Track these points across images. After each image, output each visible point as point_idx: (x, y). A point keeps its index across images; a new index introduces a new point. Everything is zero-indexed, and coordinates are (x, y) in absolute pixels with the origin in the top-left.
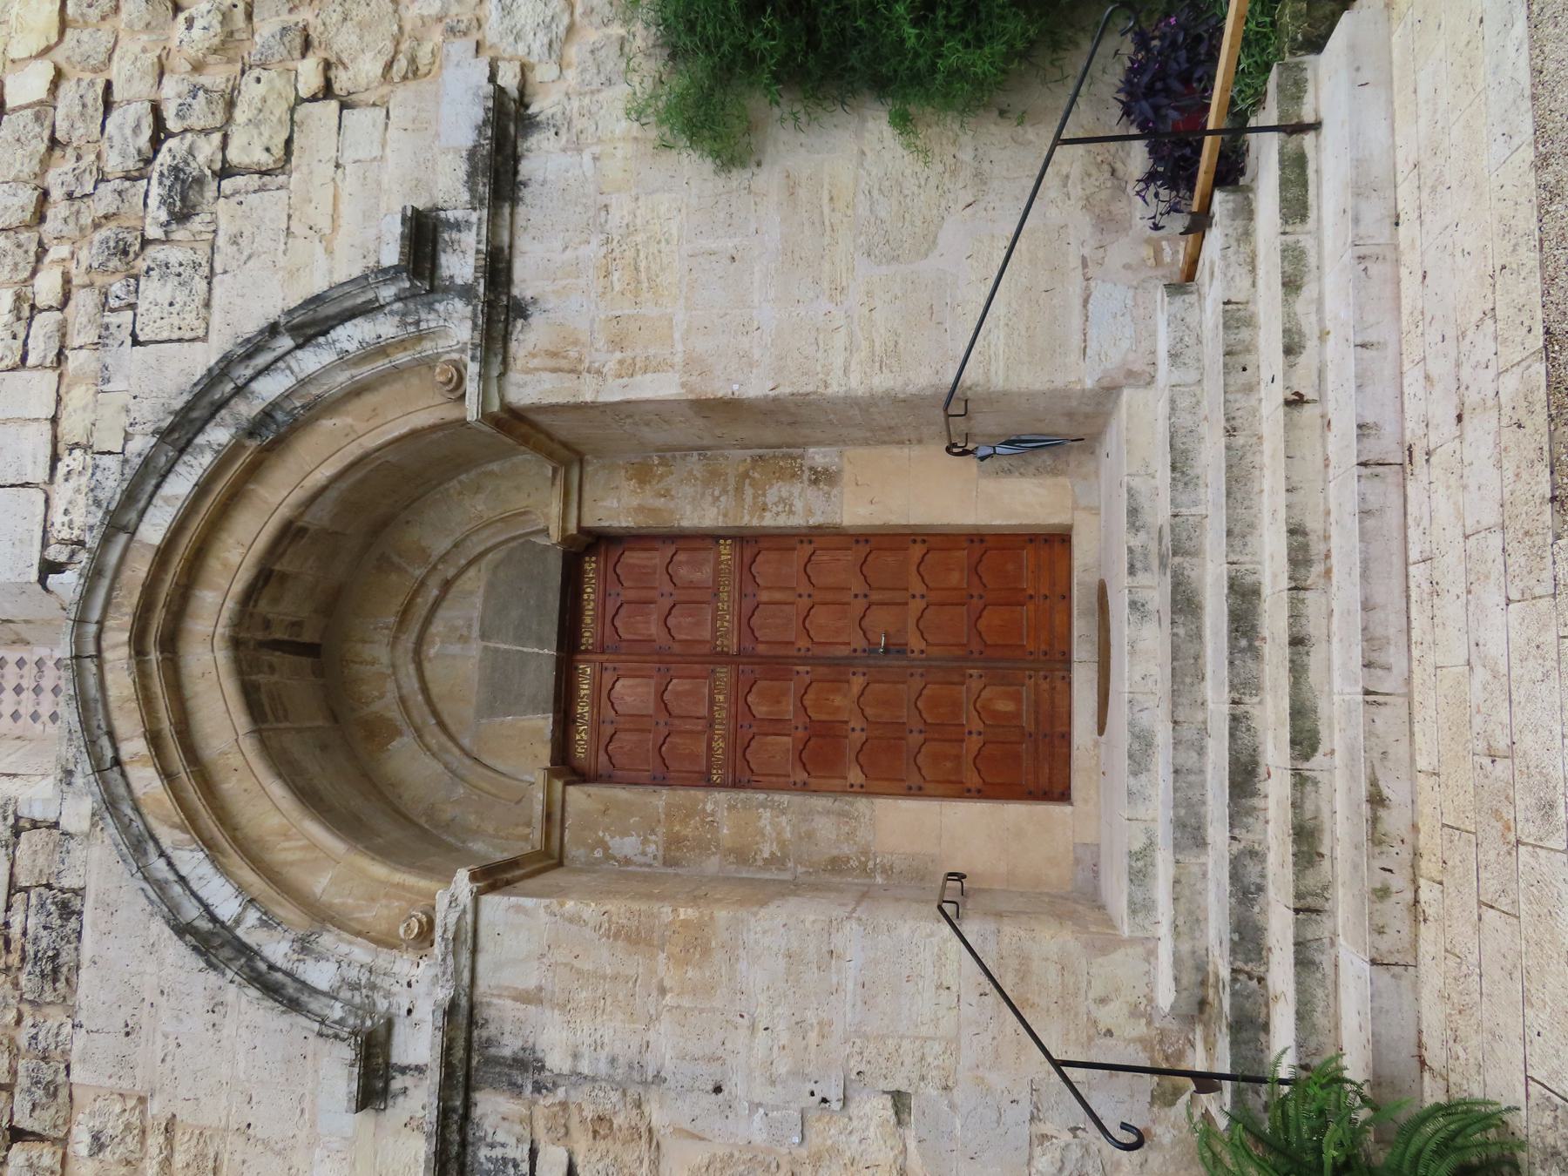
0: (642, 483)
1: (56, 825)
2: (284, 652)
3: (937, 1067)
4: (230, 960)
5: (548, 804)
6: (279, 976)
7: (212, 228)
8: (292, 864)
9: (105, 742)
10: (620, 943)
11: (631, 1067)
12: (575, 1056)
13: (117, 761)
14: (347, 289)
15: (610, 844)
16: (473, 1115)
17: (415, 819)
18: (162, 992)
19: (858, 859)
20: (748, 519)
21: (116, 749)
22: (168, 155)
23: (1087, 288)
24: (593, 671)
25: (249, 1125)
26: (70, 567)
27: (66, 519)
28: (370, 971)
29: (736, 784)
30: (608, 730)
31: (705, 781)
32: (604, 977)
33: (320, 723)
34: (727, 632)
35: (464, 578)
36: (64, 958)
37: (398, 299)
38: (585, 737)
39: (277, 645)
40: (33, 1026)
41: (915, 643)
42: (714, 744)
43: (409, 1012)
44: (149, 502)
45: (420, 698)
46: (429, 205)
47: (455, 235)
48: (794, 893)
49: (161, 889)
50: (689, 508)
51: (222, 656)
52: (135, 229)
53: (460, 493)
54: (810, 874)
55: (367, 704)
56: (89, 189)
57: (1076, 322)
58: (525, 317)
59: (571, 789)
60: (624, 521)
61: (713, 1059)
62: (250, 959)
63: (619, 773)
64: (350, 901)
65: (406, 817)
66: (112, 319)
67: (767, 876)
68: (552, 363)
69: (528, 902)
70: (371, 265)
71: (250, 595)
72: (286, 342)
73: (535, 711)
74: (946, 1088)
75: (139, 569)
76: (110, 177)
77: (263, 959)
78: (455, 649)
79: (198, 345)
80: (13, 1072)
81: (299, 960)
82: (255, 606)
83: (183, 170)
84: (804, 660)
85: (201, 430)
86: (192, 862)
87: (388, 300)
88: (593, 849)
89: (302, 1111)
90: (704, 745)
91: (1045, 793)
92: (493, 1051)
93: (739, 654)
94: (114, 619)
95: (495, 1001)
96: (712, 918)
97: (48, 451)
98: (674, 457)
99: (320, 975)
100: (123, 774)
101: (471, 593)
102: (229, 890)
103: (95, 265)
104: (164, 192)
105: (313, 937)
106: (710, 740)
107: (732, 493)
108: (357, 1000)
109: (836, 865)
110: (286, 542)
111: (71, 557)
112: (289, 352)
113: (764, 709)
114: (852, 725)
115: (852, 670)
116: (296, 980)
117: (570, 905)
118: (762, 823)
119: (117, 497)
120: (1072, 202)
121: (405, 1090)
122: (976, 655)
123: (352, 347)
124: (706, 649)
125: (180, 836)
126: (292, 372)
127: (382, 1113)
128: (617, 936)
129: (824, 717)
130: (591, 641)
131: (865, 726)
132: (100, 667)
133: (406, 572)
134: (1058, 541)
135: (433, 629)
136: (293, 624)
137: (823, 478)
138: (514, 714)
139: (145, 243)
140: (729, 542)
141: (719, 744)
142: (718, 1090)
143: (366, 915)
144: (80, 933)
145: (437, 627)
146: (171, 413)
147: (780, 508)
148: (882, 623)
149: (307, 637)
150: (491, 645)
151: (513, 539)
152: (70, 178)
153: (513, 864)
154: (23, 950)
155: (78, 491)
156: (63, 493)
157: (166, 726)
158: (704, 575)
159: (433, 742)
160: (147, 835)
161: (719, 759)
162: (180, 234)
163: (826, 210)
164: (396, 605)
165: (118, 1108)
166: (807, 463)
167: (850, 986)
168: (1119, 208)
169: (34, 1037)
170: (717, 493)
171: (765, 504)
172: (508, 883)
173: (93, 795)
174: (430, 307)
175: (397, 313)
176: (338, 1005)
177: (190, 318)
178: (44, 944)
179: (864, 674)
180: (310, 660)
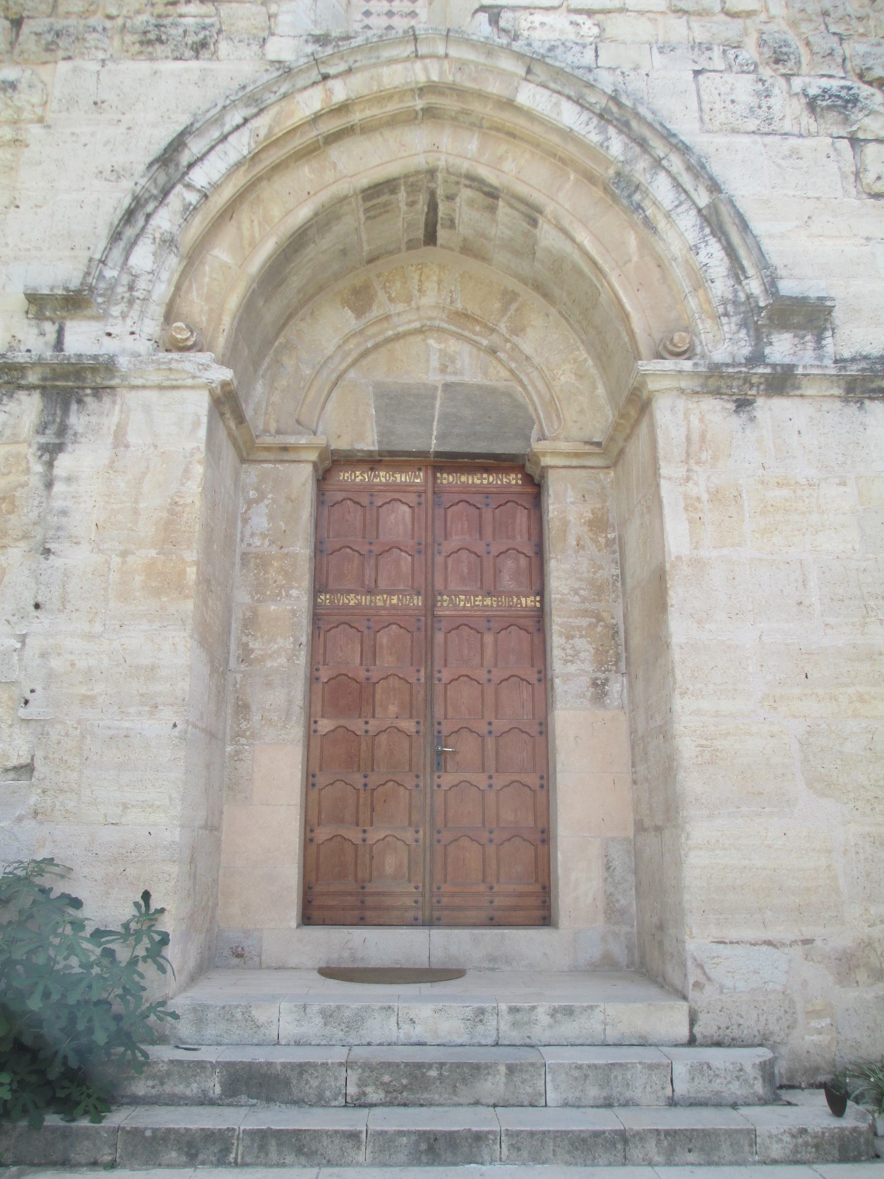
0: (590, 524)
1: (273, 34)
2: (427, 214)
3: (55, 806)
4: (155, 180)
5: (296, 448)
6: (141, 222)
7: (803, 132)
8: (239, 228)
9: (343, 67)
10: (165, 515)
11: (59, 528)
12: (69, 480)
13: (326, 77)
14: (755, 251)
15: (262, 504)
16: (20, 392)
17: (283, 333)
18: (129, 128)
19: (248, 729)
20: (557, 623)
21: (335, 77)
22: (868, 93)
23: (783, 944)
24: (417, 485)
25: (17, 207)
26: (495, 30)
27: (537, 24)
28: (144, 299)
29: (317, 617)
30: (365, 500)
31: (319, 587)
32: (136, 502)
33: (366, 248)
34: (455, 605)
35: (500, 367)
36: (159, 48)
37: (749, 297)
38: (358, 480)
39: (433, 207)
40: (104, 29)
41: (448, 779)
42: (352, 595)
43: (109, 334)
44: (554, 91)
45: (390, 333)
46: (837, 322)
47: (810, 345)
48: (214, 671)
49: (216, 120)
50: (567, 566)
51: (420, 161)
52: (799, 68)
53: (575, 360)
54: (235, 686)
55: (384, 288)
56: (833, 29)
57: (749, 934)
58: (736, 411)
59: (309, 468)
60: (553, 508)
61: (64, 601)
62: (155, 198)
63: (326, 512)
64: (207, 280)
65: (284, 325)
66: (716, 53)
67: (233, 647)
68: (695, 437)
69: (202, 432)
70: (778, 272)
71: (474, 181)
72: (703, 199)
73: (381, 434)
74: (36, 813)
75: (494, 87)
76: (845, 45)
77: (156, 208)
78: (435, 363)
79: (697, 125)
80: (68, 14)
81: (154, 239)
82: (466, 186)
83: (855, 106)
84: (430, 677)
85: (620, 132)
87: (746, 287)
88: (256, 489)
89: (29, 250)
90: (352, 587)
91: (310, 902)
92: (74, 407)
93: (434, 616)
94: (450, 68)
95: (117, 408)
96: (187, 597)
97: (596, 6)
98: (614, 552)
100: (314, 84)
101: (485, 374)
102: (215, 177)
103: (765, 37)
104: (834, 91)
105: (175, 250)
106: (357, 593)
107: (583, 606)
108: (120, 290)
109: (243, 709)
110: (522, 208)
111: (504, 30)
112: (694, 203)
113: (385, 641)
114: (372, 722)
115: (422, 721)
116: (138, 236)
117: (199, 470)
118: (280, 640)
119: (557, 64)
120: (867, 930)
121: (43, 334)
122: (436, 836)
123: (702, 257)
124: (439, 585)
125: (263, 133)
126: (677, 206)
127: (24, 315)
128: (171, 512)
129: (378, 696)
130: (445, 482)
131: (370, 734)
132: (407, 59)
133: (503, 316)
135: (452, 341)
136: (452, 221)
137: (599, 689)
138: (377, 416)
139: (787, 77)
140: (538, 605)
141: (352, 600)
142: (37, 606)
143: (195, 293)
144: (181, 59)
145: (453, 346)
146: (634, 104)
147: (569, 651)
148: (467, 747)
149: (442, 234)
150: (439, 393)
151: (536, 410)
152: (840, 12)
153: (240, 419)
154: (168, 16)
155: (562, 32)
156: (560, 22)
157: (357, 116)
158: (507, 582)
159: (351, 345)
160: (262, 106)
161: (339, 601)
162: (798, 106)
163: (851, 690)
164: (473, 308)
165: (35, 100)
166: (612, 676)
167: (127, 724)
168: (862, 975)
169: (95, 30)
170: (582, 592)
171: (573, 637)
172: (222, 415)
173: (297, 60)
174: (743, 324)
175: (736, 296)
176: (115, 273)
177: (721, 118)
178: (173, 31)
179: (418, 732)
180: (422, 237)
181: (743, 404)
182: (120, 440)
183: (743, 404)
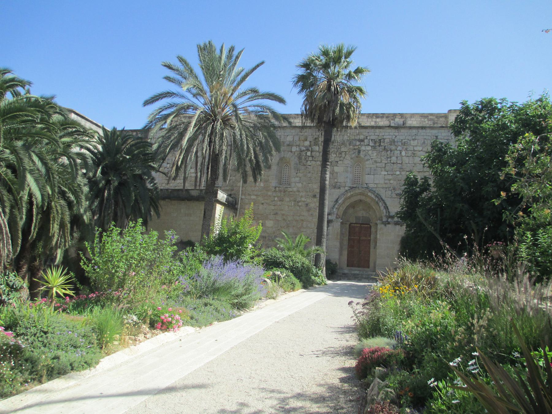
20: (371, 241)
29: (349, 239)
31: (349, 236)
86: (343, 199)
99: (334, 210)
134: (368, 267)
181: (385, 225)
182: (333, 227)
183: (385, 225)
